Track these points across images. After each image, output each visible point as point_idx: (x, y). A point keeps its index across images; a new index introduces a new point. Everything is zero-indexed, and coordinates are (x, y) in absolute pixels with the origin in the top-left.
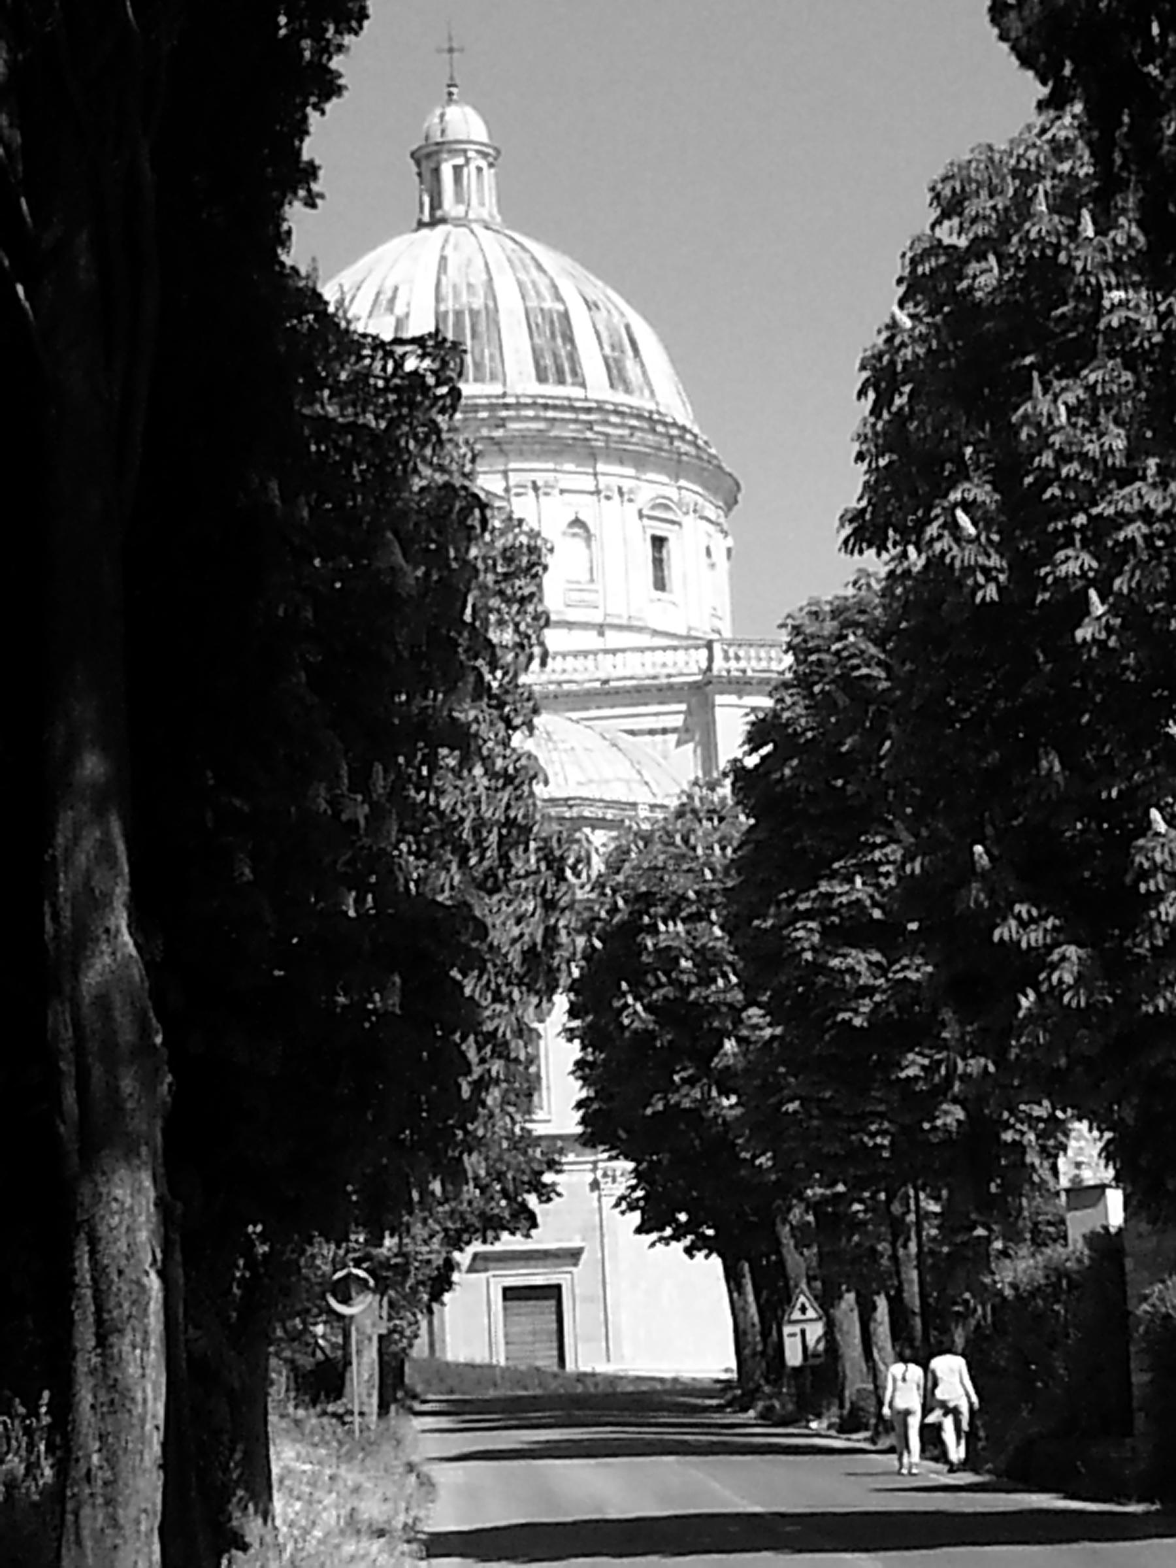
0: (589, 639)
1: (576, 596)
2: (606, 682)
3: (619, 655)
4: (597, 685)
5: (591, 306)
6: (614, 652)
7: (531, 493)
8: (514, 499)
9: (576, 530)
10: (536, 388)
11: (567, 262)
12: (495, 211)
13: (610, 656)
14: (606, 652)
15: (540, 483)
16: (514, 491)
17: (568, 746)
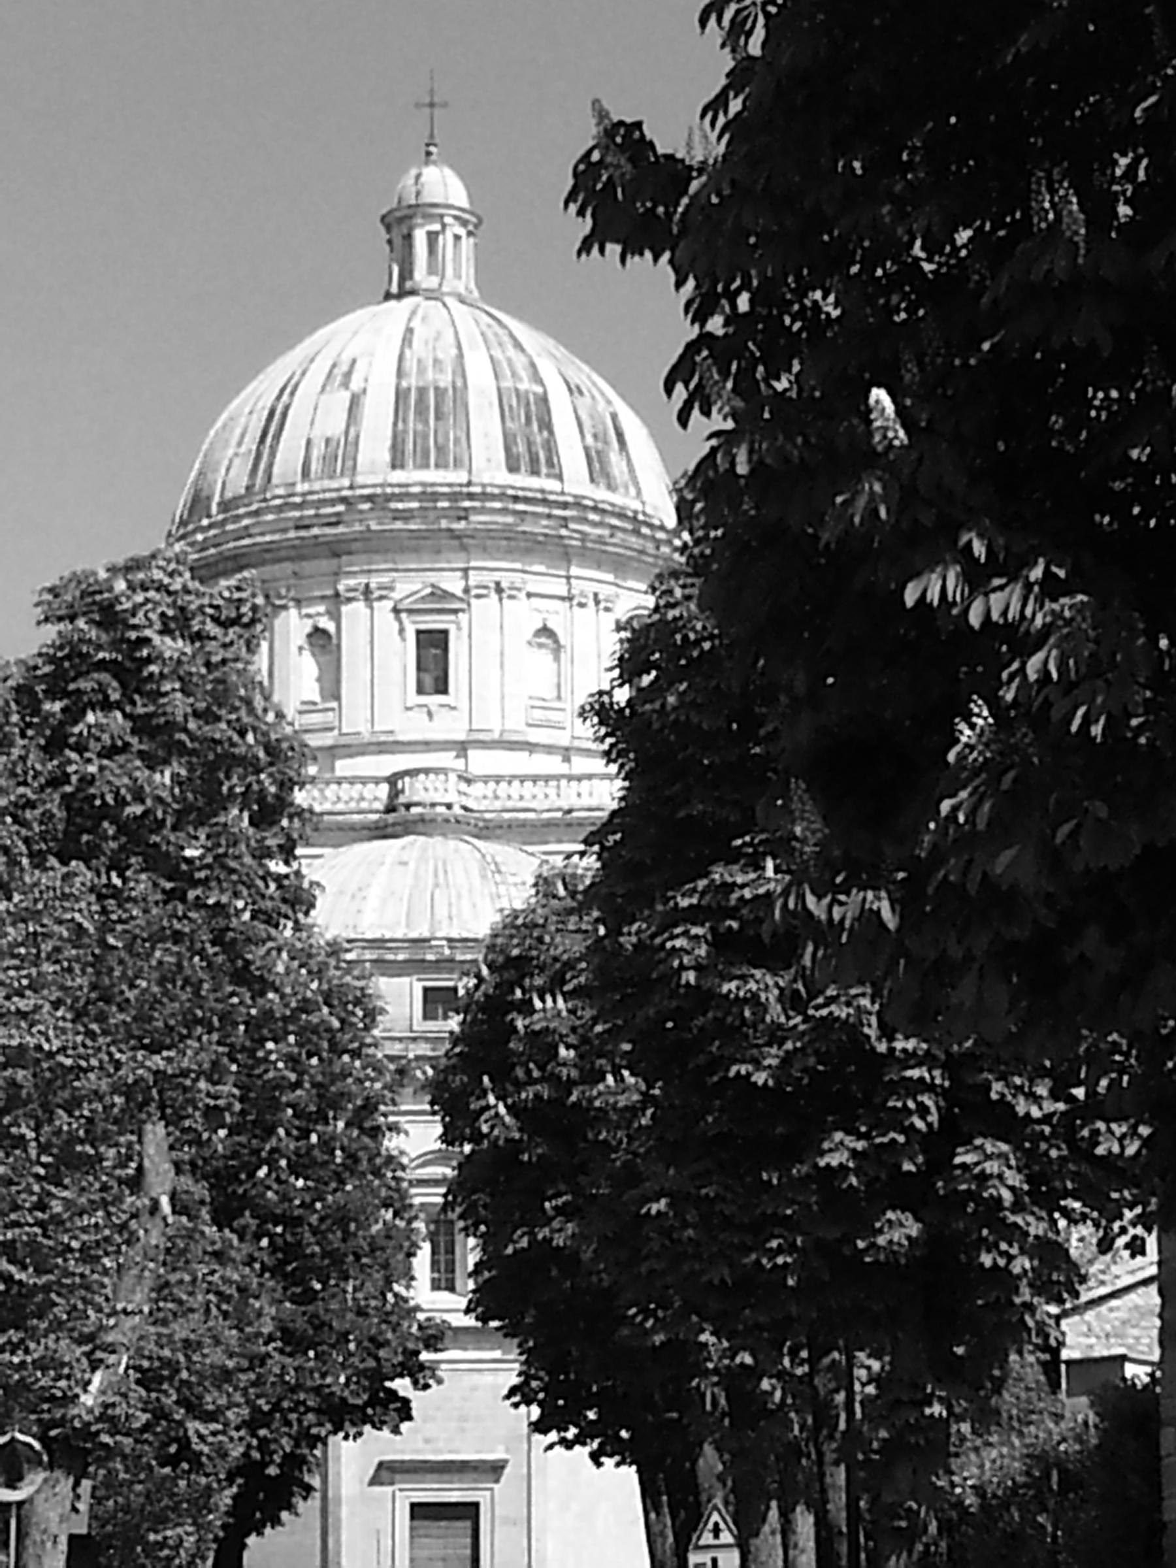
0: (552, 764)
1: (538, 714)
2: (570, 811)
3: (585, 783)
4: (559, 814)
5: (574, 390)
6: (579, 779)
7: (494, 596)
8: (473, 601)
9: (543, 640)
10: (503, 477)
11: (551, 343)
12: (472, 285)
13: (574, 783)
14: (570, 778)
15: (504, 585)
16: (474, 592)
17: (518, 880)
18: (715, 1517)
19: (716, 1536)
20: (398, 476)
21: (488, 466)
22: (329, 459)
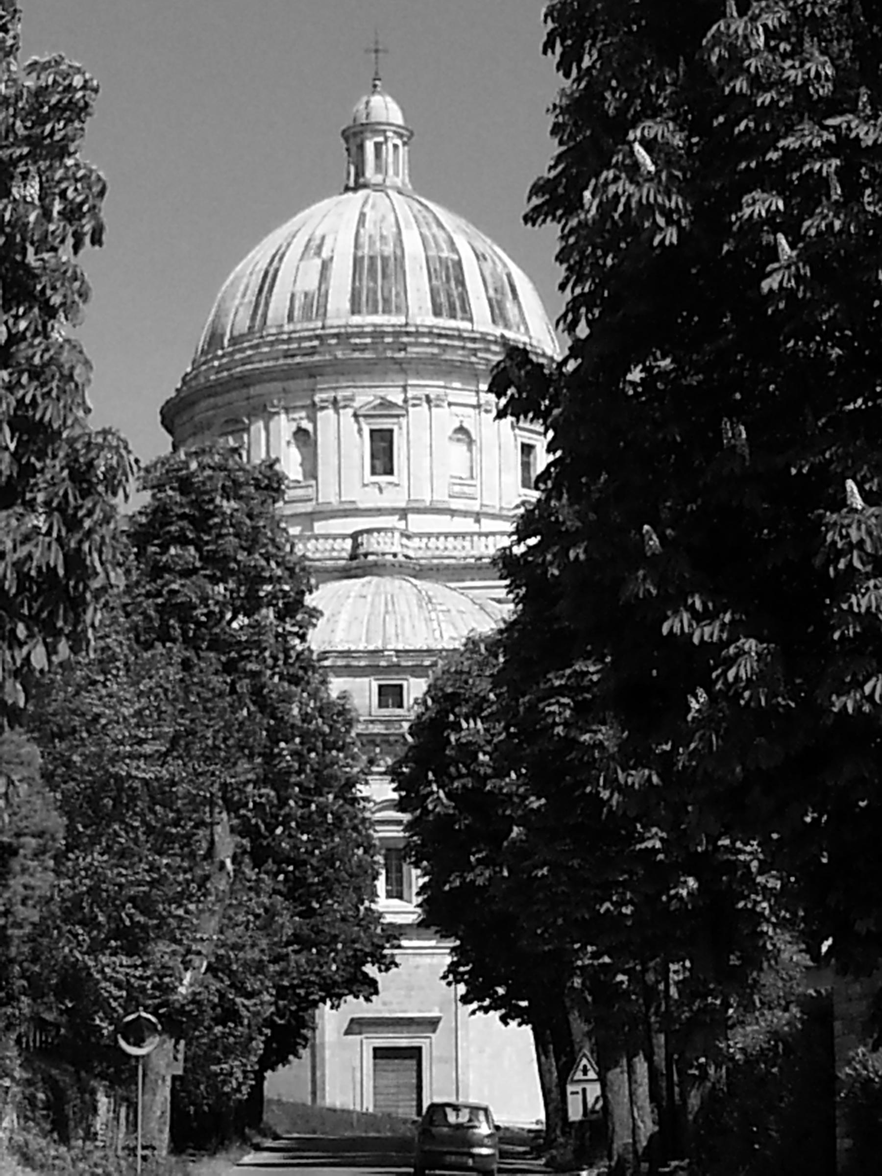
0: (467, 525)
1: (457, 489)
2: (480, 558)
3: (491, 538)
4: (472, 561)
5: (480, 257)
6: (487, 535)
7: (425, 405)
8: (411, 409)
9: (460, 436)
10: (430, 320)
11: (462, 222)
12: (407, 180)
13: (483, 538)
14: (480, 535)
15: (432, 396)
16: (411, 402)
17: (444, 608)
18: (584, 1062)
19: (585, 1073)
20: (356, 320)
21: (420, 313)
22: (307, 307)
